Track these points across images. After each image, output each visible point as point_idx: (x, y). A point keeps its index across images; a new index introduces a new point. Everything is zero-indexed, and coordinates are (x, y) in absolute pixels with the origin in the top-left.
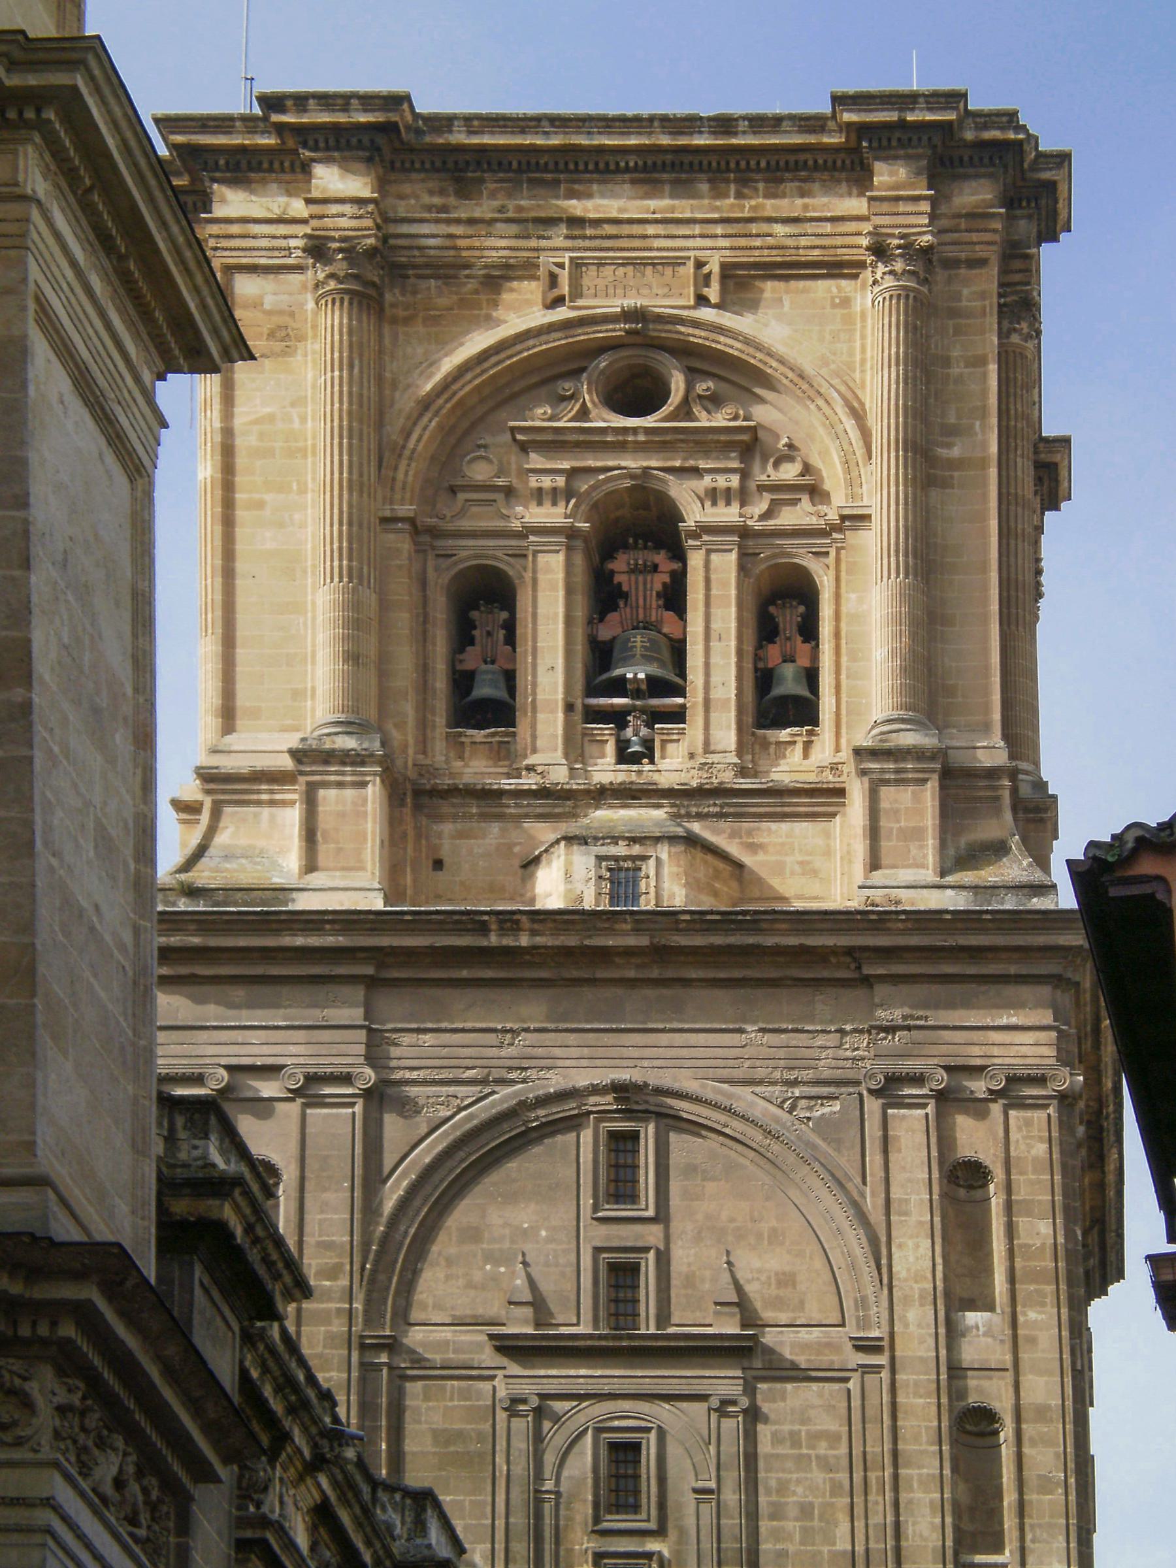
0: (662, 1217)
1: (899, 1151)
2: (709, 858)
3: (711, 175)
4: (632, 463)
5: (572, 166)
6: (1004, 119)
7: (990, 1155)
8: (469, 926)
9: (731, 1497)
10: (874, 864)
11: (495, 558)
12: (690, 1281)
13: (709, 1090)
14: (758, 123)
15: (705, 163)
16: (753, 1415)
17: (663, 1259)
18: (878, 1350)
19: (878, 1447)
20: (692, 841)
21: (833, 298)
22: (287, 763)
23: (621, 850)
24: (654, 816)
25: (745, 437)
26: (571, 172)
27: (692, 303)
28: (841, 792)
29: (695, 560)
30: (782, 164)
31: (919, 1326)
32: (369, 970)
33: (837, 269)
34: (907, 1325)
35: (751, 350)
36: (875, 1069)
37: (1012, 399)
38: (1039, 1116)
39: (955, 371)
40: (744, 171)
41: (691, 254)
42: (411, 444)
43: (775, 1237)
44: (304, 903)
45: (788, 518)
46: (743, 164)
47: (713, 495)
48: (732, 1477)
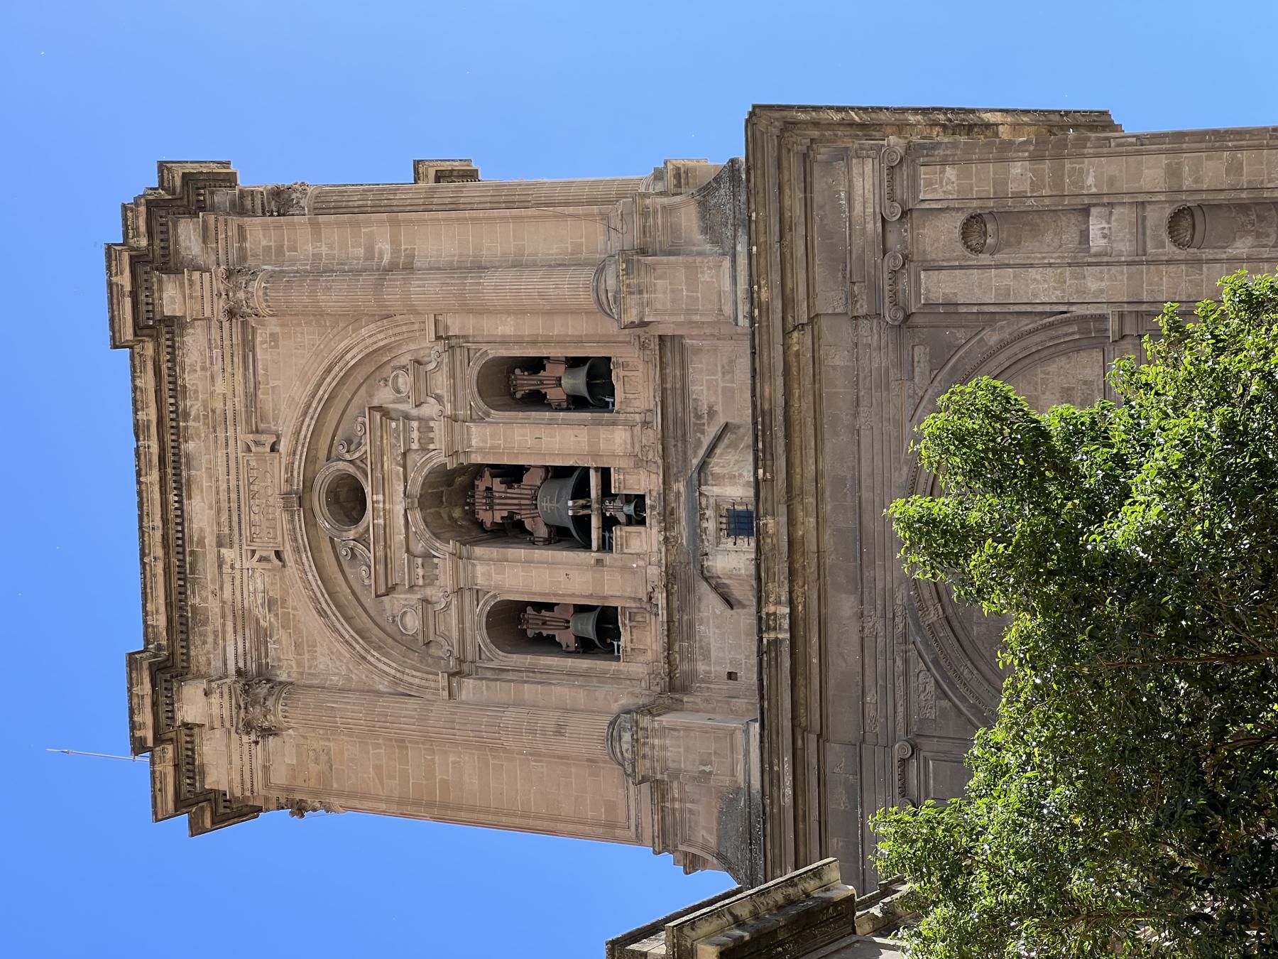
1: (955, 294)
2: (718, 451)
3: (181, 440)
5: (180, 542)
6: (129, 214)
8: (773, 654)
11: (480, 615)
15: (173, 444)
21: (271, 347)
23: (711, 526)
25: (378, 416)
26: (184, 543)
27: (277, 455)
30: (171, 386)
31: (1102, 280)
32: (813, 738)
34: (1101, 291)
35: (311, 410)
37: (351, 204)
39: (324, 250)
40: (177, 416)
41: (240, 455)
42: (393, 672)
45: (441, 383)
46: (173, 416)
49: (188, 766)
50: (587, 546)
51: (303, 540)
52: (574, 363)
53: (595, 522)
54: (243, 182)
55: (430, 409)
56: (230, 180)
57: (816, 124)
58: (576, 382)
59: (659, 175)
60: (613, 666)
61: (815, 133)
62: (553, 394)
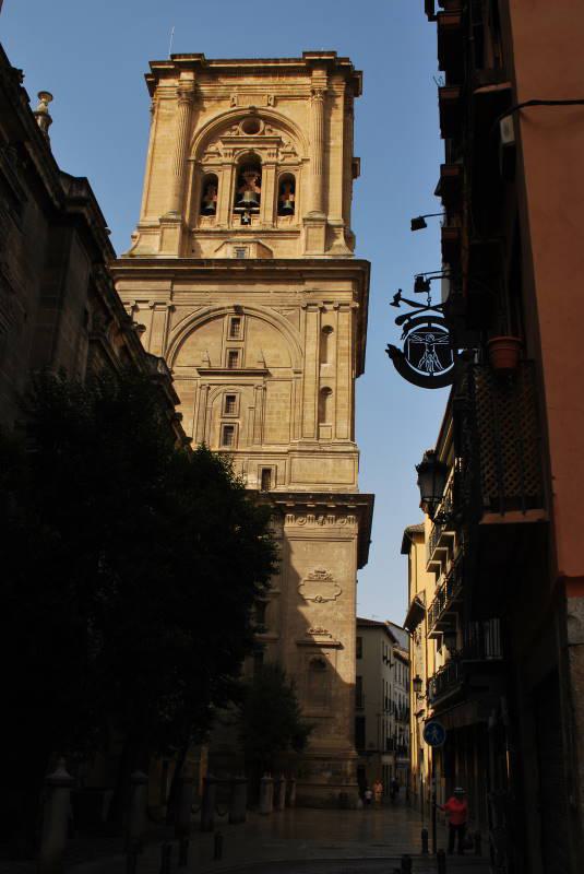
4: (250, 146)
9: (258, 409)
10: (306, 249)
12: (251, 357)
13: (260, 308)
14: (285, 60)
16: (265, 389)
18: (300, 373)
19: (299, 396)
20: (259, 243)
22: (158, 223)
23: (241, 245)
24: (251, 237)
28: (299, 232)
29: (264, 172)
33: (303, 97)
38: (346, 314)
43: (275, 346)
44: (159, 257)
45: (287, 161)
47: (269, 155)
48: (259, 405)
49: (167, 74)
50: (236, 205)
51: (239, 113)
52: (293, 204)
53: (243, 209)
54: (356, 99)
55: (281, 157)
56: (357, 95)
57: (364, 282)
58: (288, 205)
59: (351, 232)
60: (197, 213)
61: (361, 282)
62: (283, 197)
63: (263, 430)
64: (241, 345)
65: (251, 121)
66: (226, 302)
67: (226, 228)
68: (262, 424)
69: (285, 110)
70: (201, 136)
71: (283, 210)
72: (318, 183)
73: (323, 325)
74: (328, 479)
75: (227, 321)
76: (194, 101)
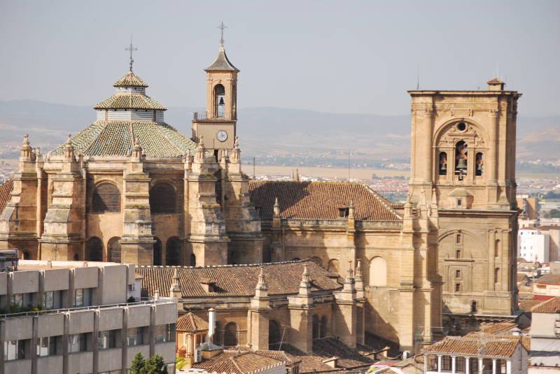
0: (463, 245)
4: (461, 138)
7: (500, 239)
10: (489, 201)
17: (463, 249)
36: (488, 229)
63: (472, 286)
64: (462, 247)
65: (462, 126)
66: (455, 228)
67: (452, 184)
68: (472, 283)
69: (476, 119)
70: (438, 133)
71: (478, 173)
72: (494, 165)
73: (497, 239)
74: (499, 308)
75: (455, 236)
76: (433, 114)
